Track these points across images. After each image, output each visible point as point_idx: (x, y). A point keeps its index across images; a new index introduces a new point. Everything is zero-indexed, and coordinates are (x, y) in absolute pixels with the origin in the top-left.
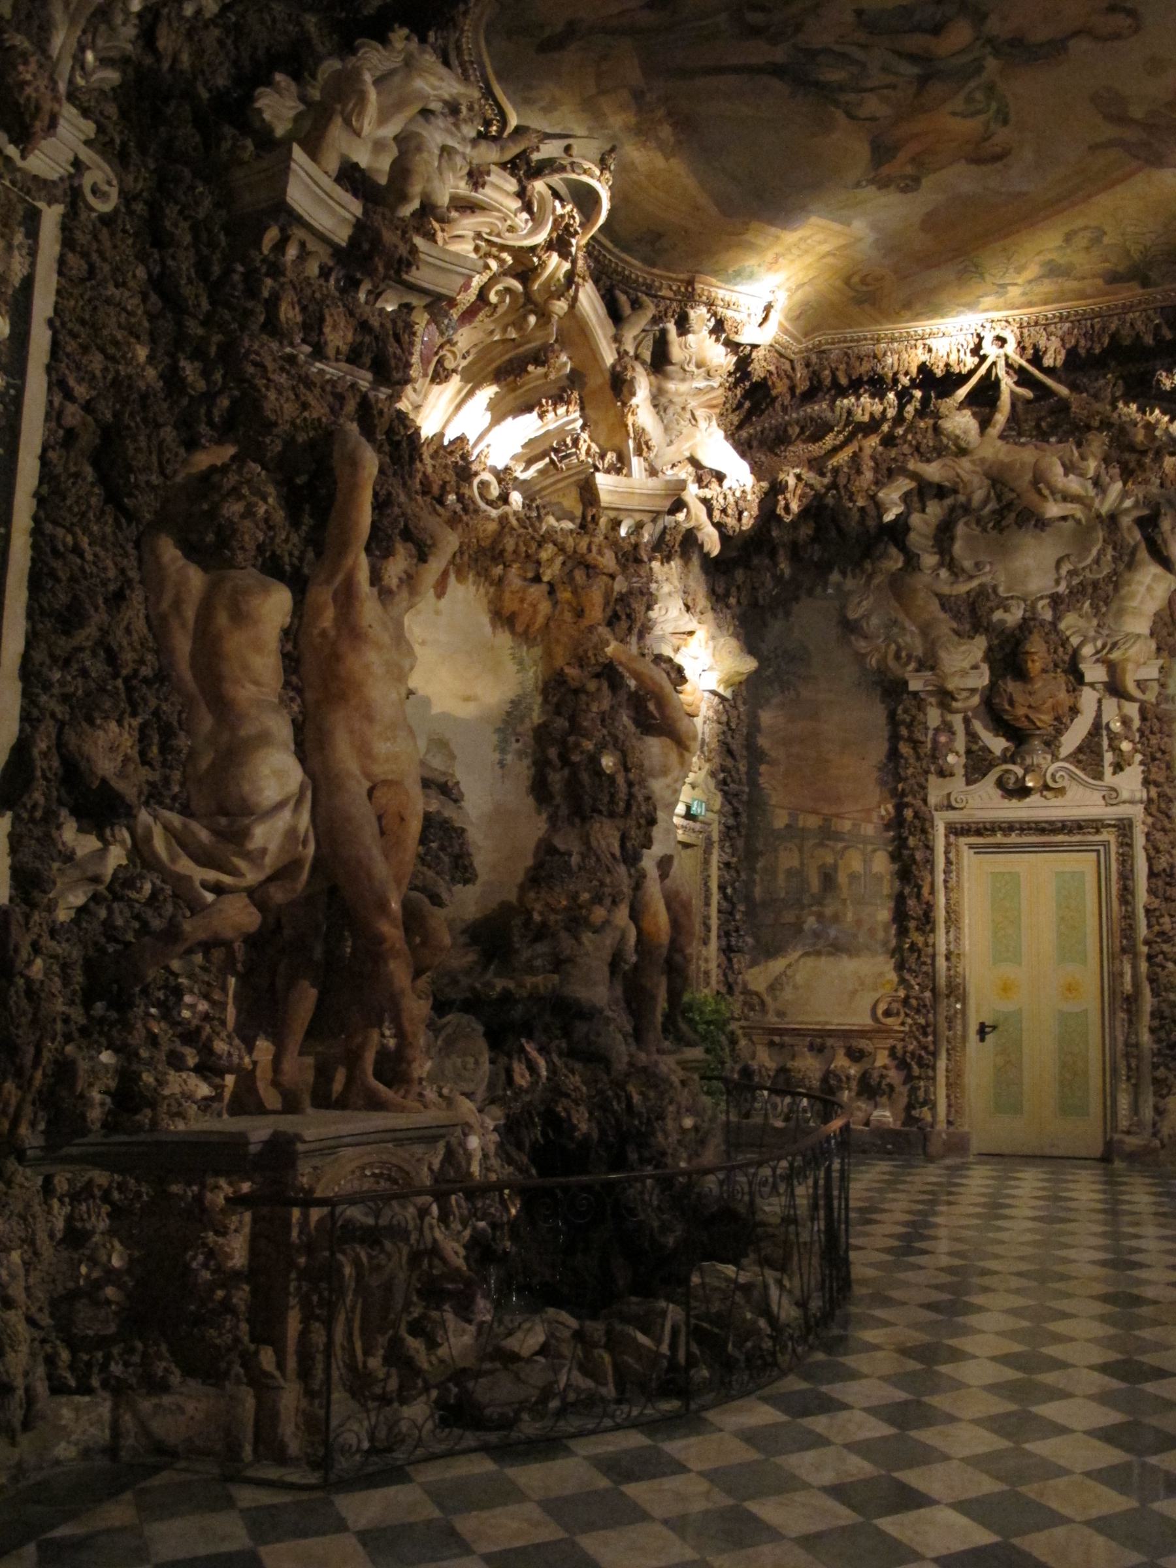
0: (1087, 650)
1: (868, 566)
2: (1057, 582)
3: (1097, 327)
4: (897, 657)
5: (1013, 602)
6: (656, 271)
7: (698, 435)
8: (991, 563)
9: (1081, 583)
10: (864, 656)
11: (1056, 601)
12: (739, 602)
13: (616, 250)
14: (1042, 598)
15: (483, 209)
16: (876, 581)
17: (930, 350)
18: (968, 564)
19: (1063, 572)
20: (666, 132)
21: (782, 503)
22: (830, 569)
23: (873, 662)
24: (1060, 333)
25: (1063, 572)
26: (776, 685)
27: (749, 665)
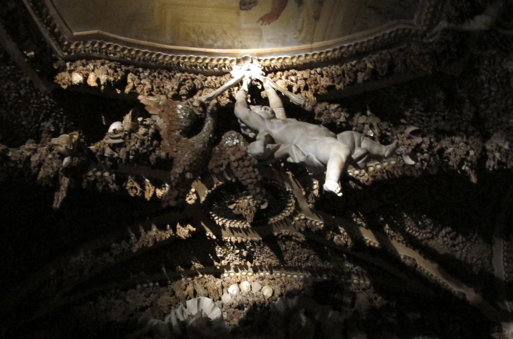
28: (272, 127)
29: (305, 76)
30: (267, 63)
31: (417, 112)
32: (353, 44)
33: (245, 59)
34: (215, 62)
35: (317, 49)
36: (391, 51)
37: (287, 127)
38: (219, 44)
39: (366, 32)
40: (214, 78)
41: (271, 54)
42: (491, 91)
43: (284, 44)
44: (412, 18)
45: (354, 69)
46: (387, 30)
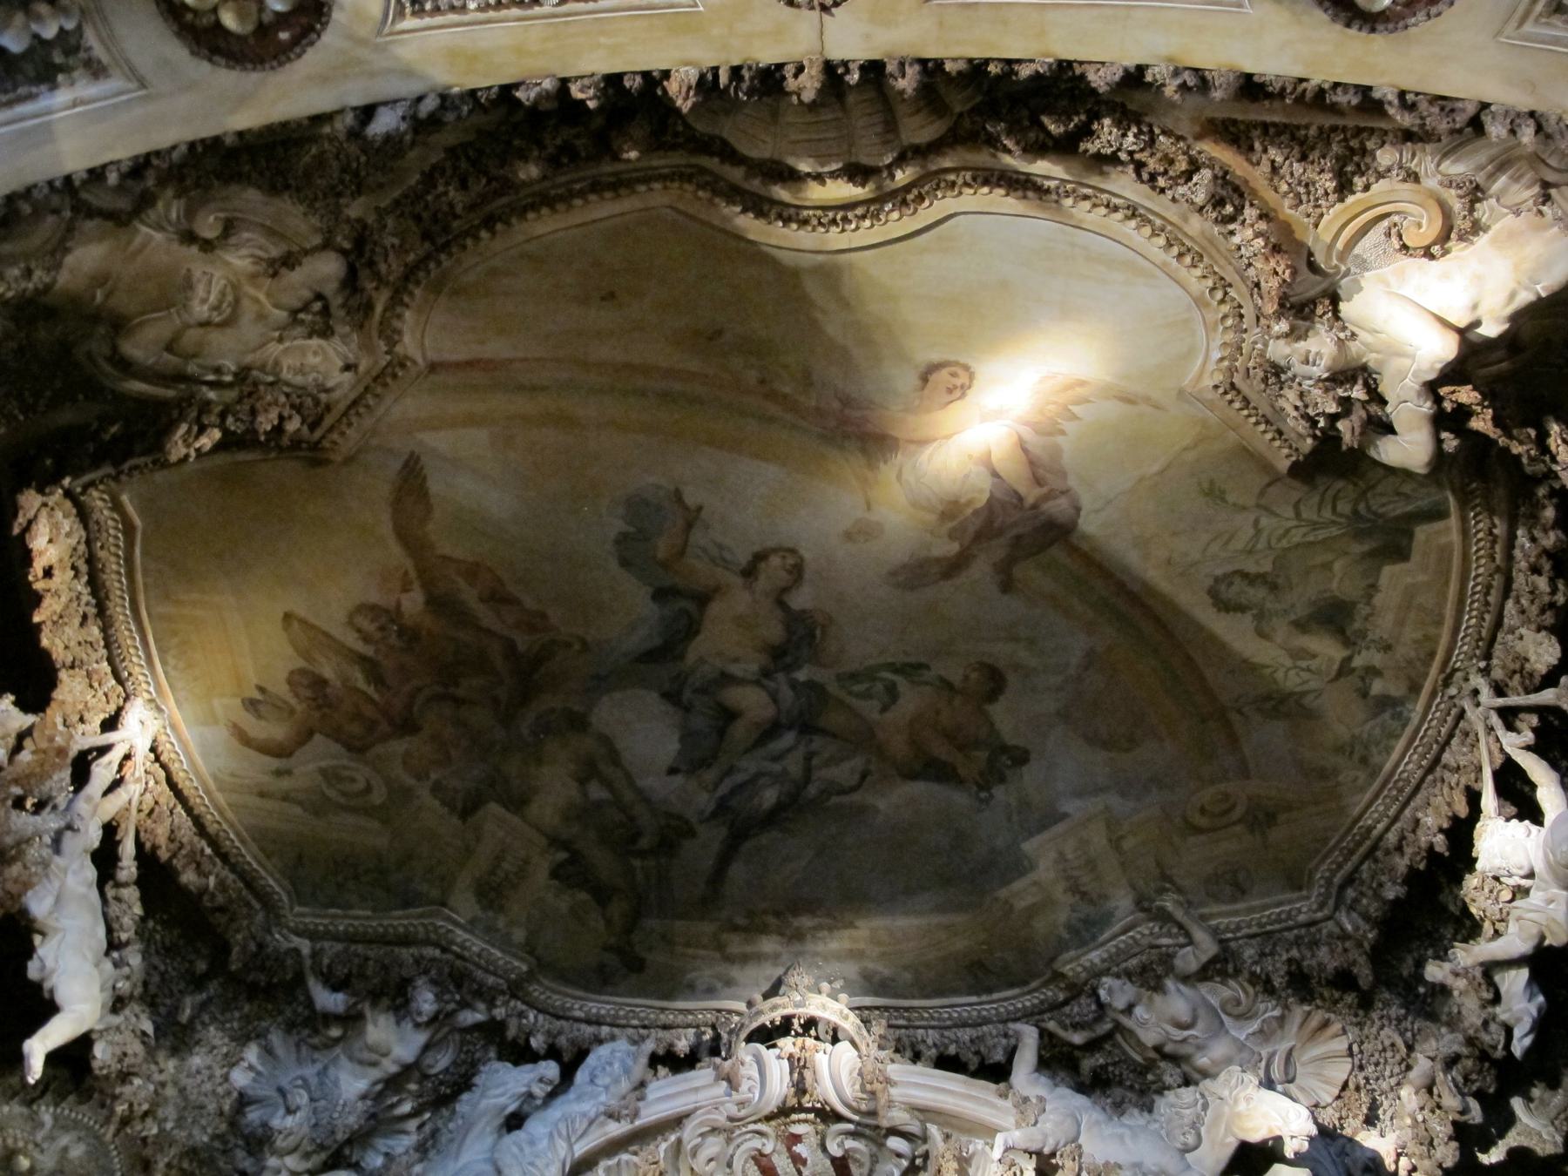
6: (1034, 985)
7: (1226, 1109)
13: (984, 998)
15: (687, 1115)
20: (806, 922)
28: (75, 873)
29: (162, 800)
30: (163, 738)
31: (158, 937)
32: (237, 844)
33: (159, 709)
34: (137, 670)
35: (211, 800)
36: (244, 892)
37: (85, 897)
38: (173, 673)
39: (261, 856)
40: (108, 670)
41: (180, 740)
42: (230, 1021)
43: (204, 755)
44: (300, 904)
45: (198, 858)
46: (272, 882)
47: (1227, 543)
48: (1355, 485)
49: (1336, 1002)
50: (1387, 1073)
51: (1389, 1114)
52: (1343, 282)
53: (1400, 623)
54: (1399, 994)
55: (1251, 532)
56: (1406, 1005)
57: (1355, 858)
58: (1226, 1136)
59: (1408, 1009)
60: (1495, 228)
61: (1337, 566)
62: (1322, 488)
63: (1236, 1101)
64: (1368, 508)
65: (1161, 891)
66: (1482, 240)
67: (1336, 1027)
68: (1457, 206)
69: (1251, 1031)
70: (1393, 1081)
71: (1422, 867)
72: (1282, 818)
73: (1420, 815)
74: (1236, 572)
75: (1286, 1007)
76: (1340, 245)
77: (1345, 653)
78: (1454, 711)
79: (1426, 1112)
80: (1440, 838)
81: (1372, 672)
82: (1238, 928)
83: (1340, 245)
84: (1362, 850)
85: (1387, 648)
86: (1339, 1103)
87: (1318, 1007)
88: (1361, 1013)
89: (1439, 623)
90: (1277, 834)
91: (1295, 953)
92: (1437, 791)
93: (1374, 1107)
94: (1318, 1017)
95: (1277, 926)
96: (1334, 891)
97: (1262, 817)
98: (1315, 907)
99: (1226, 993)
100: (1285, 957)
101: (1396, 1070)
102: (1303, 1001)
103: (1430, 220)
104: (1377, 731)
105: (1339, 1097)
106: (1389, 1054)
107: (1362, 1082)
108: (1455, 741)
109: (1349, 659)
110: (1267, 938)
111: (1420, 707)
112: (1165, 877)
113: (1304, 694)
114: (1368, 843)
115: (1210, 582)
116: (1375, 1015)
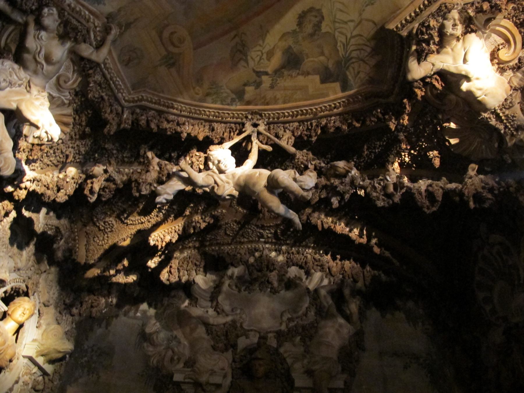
0: (297, 366)
1: (166, 301)
2: (281, 324)
3: (314, 124)
4: (172, 359)
5: (252, 333)
8: (241, 309)
9: (296, 326)
10: (150, 357)
11: (279, 334)
12: (80, 314)
14: (270, 332)
16: (168, 312)
17: (213, 130)
18: (227, 308)
19: (285, 318)
21: (90, 185)
22: (142, 302)
23: (154, 361)
24: (291, 128)
25: (285, 318)
26: (86, 370)
27: (68, 346)
47: (341, 11)
48: (367, 56)
49: (80, 125)
50: (51, 159)
51: (33, 168)
52: (480, 32)
53: (285, 89)
54: (92, 148)
55: (346, 20)
56: (87, 153)
57: (157, 107)
58: (15, 101)
59: (85, 154)
60: (502, 77)
61: (322, 58)
62: (368, 44)
63: (37, 99)
64: (353, 63)
65: (120, 26)
66: (498, 75)
67: (68, 130)
68: (511, 64)
69: (51, 93)
70: (49, 163)
71: (169, 133)
72: (173, 70)
73: (187, 124)
74: (323, 18)
75: (69, 104)
76: (498, 28)
77: (270, 72)
78: (239, 120)
79: (73, 181)
80: (186, 135)
81: (258, 85)
82: (107, 69)
83: (498, 28)
84: (161, 108)
85: (272, 87)
86: (30, 146)
87: (75, 119)
88: (78, 137)
89: (284, 102)
90: (163, 70)
91: (106, 98)
92: (200, 126)
93: (35, 161)
94: (70, 120)
95: (113, 86)
96: (138, 103)
97: (171, 61)
98: (126, 98)
99: (70, 75)
100: (103, 94)
101: (55, 162)
102: (76, 111)
103: (509, 56)
104: (225, 95)
105: (33, 145)
106: (61, 156)
107: (46, 151)
108: (223, 125)
109: (266, 73)
110: (106, 84)
111: (239, 107)
112: (128, 25)
113: (247, 61)
114: (165, 109)
115: (318, 7)
116: (78, 143)
